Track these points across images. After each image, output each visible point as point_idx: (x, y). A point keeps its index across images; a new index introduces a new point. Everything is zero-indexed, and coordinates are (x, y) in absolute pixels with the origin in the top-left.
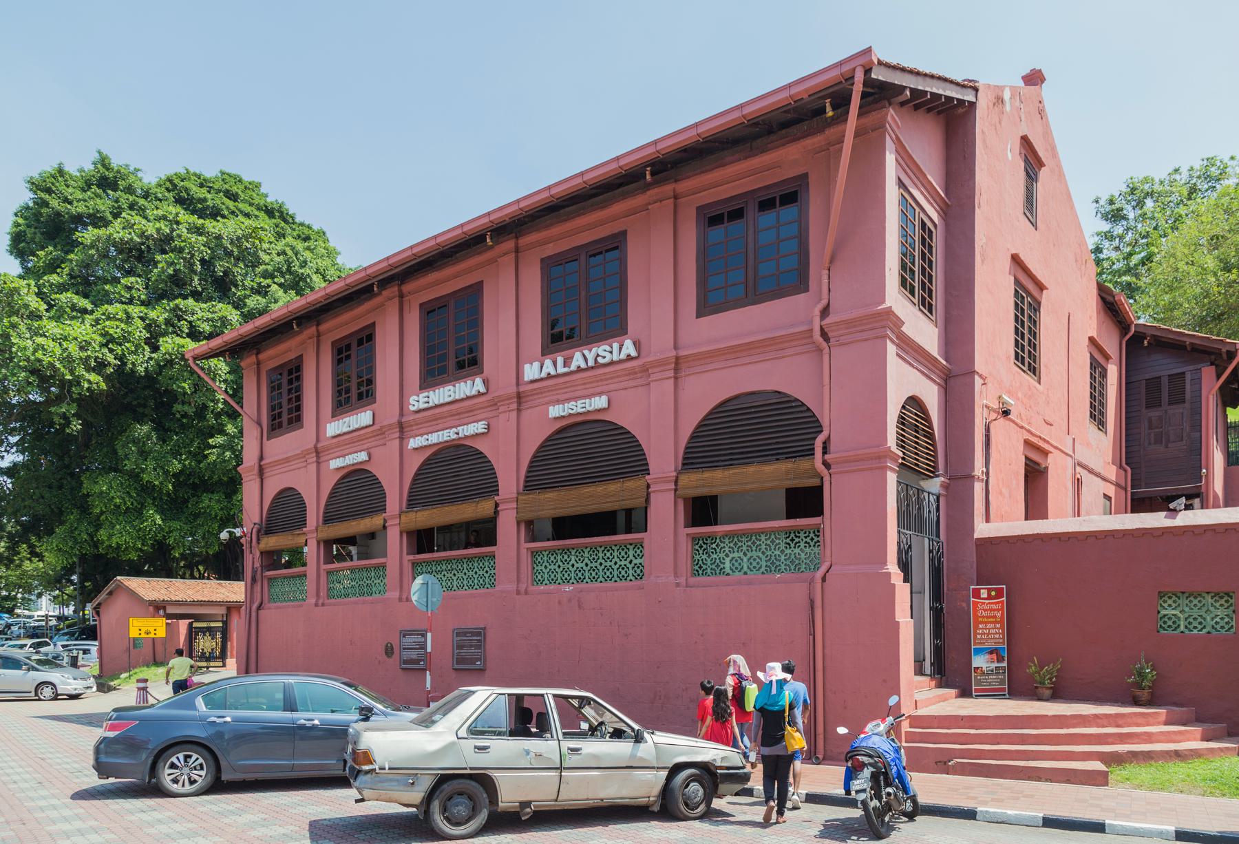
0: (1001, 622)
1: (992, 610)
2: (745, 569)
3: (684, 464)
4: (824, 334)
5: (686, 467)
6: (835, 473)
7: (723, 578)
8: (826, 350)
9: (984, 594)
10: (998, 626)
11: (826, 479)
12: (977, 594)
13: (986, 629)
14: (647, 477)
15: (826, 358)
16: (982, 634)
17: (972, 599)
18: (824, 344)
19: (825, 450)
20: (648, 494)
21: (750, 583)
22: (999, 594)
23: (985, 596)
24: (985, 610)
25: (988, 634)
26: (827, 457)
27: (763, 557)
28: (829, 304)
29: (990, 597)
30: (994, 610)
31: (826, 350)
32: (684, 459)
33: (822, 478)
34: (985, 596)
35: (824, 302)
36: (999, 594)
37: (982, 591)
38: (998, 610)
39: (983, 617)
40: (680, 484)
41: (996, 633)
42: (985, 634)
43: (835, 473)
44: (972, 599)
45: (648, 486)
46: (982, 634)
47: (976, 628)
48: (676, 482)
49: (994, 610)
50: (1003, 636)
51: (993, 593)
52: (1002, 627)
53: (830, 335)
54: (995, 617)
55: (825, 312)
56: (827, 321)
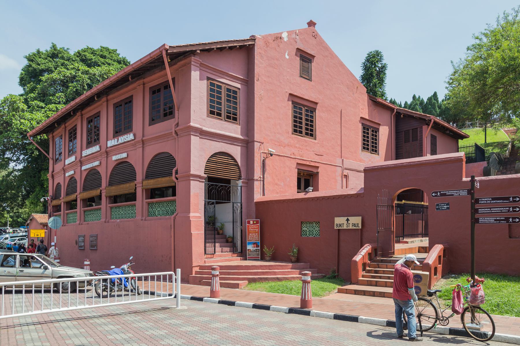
0: (258, 233)
1: (254, 228)
2: (161, 214)
3: (146, 177)
4: (176, 133)
5: (147, 178)
6: (179, 181)
7: (155, 217)
8: (177, 139)
9: (251, 222)
10: (257, 234)
11: (177, 183)
12: (249, 222)
13: (252, 235)
14: (135, 182)
15: (177, 141)
16: (250, 237)
17: (247, 224)
18: (176, 137)
19: (177, 173)
20: (136, 188)
21: (160, 219)
22: (257, 223)
23: (252, 223)
24: (252, 228)
25: (253, 237)
26: (176, 176)
27: (165, 210)
28: (178, 123)
29: (254, 224)
30: (255, 228)
31: (177, 139)
32: (146, 175)
33: (176, 183)
34: (252, 223)
35: (176, 122)
36: (257, 223)
37: (251, 221)
38: (257, 228)
39: (251, 231)
40: (144, 184)
41: (256, 237)
42: (252, 237)
43: (179, 181)
44: (247, 224)
45: (136, 185)
46: (250, 237)
47: (249, 235)
48: (142, 184)
49: (255, 228)
50: (259, 239)
51: (255, 222)
52: (258, 235)
53: (178, 133)
54: (256, 231)
55: (177, 125)
56: (178, 128)
